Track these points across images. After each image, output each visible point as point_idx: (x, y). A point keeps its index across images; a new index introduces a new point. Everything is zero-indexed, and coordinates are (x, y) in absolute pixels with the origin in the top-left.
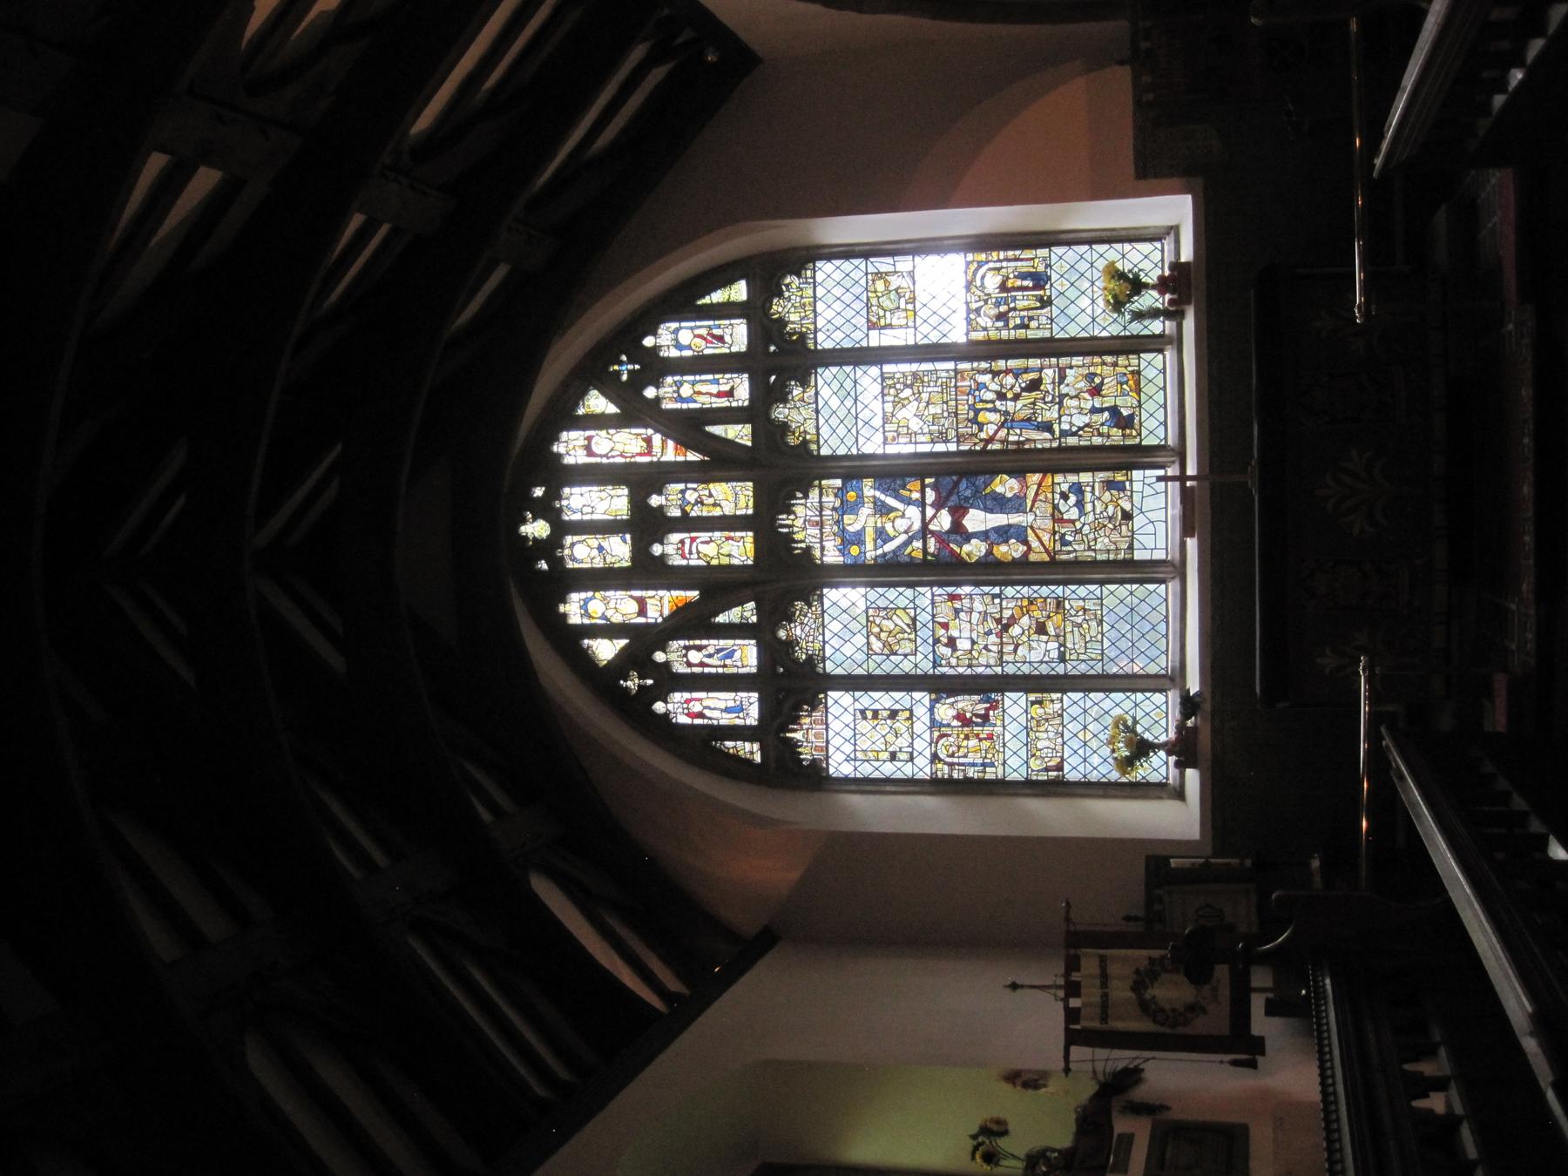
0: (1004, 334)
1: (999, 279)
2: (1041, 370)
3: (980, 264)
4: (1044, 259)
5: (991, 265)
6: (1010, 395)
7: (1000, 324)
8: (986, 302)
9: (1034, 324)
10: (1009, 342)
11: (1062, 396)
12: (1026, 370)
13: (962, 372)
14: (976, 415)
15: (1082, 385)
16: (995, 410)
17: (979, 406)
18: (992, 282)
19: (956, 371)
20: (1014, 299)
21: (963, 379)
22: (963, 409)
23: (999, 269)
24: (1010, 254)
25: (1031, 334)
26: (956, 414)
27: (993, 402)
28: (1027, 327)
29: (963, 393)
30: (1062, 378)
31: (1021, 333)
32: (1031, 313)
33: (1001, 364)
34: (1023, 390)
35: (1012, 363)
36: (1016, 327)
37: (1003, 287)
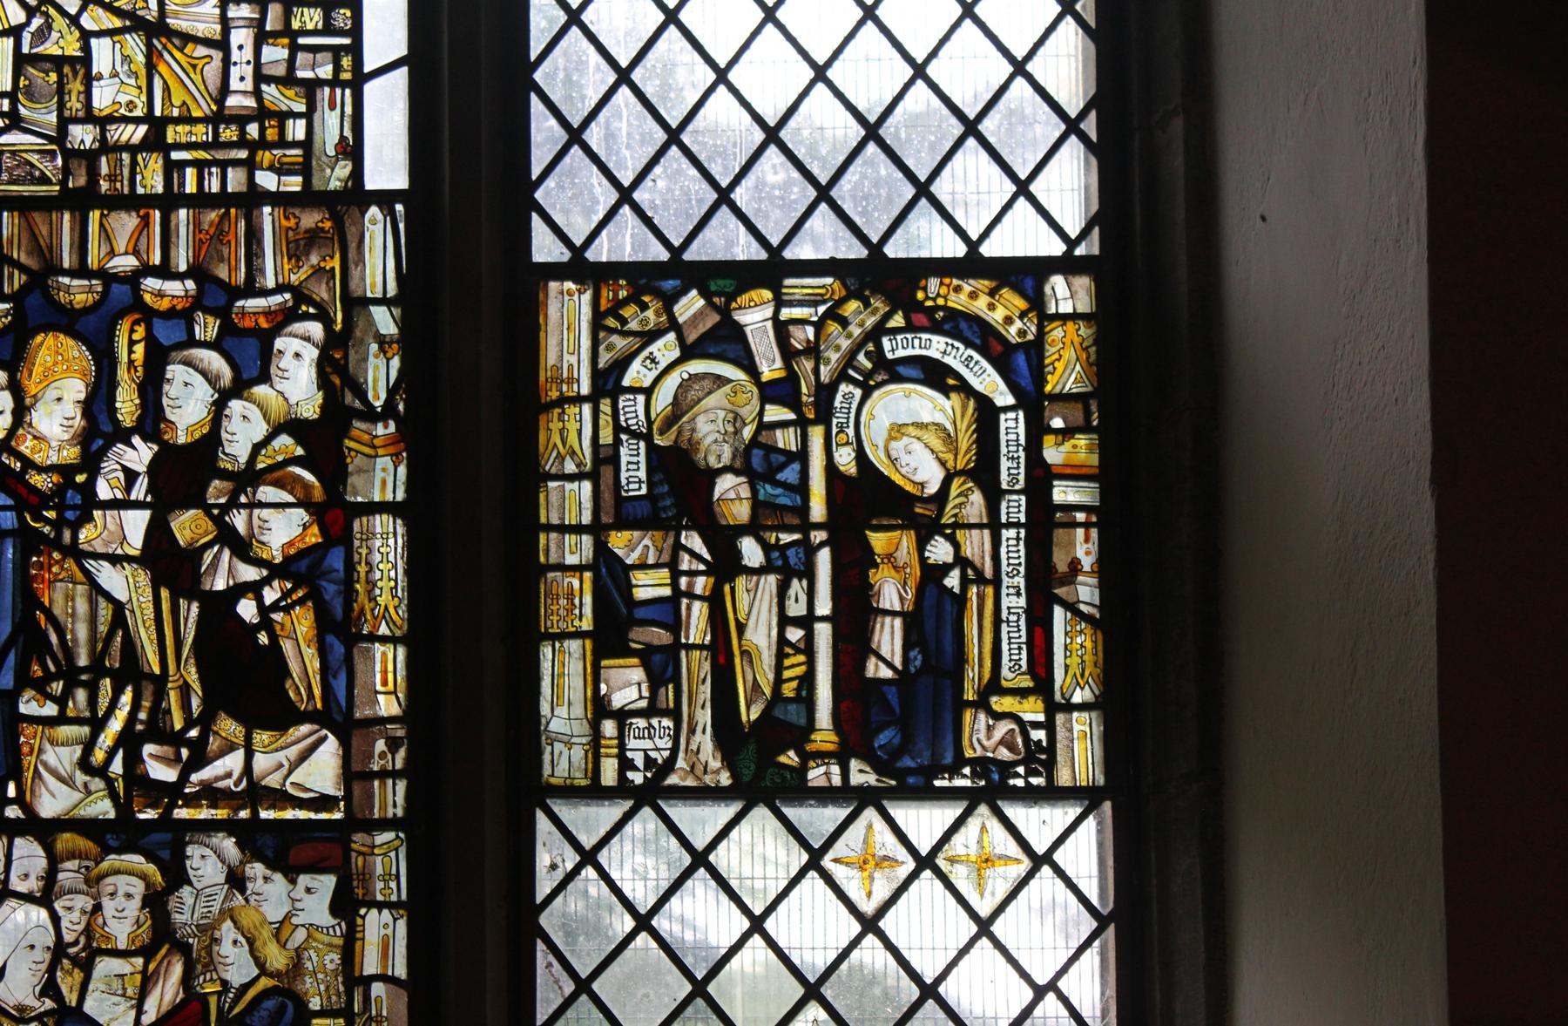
0: (573, 500)
1: (921, 468)
2: (341, 718)
3: (1022, 363)
4: (1042, 757)
5: (1012, 427)
6: (187, 526)
7: (634, 470)
8: (780, 391)
9: (627, 685)
10: (524, 524)
11: (168, 850)
12: (342, 632)
13: (346, 242)
14: (67, 321)
15: (236, 965)
16: (99, 429)
17: (129, 346)
18: (907, 431)
19: (356, 196)
20: (789, 568)
21: (297, 246)
22: (117, 242)
23: (984, 472)
24: (1083, 548)
25: (563, 674)
26: (81, 201)
27: (152, 421)
28: (609, 640)
29: (209, 244)
30: (285, 847)
31: (575, 603)
32: (696, 667)
33: (383, 478)
34: (219, 607)
35: (385, 549)
36: (610, 574)
37: (869, 497)
